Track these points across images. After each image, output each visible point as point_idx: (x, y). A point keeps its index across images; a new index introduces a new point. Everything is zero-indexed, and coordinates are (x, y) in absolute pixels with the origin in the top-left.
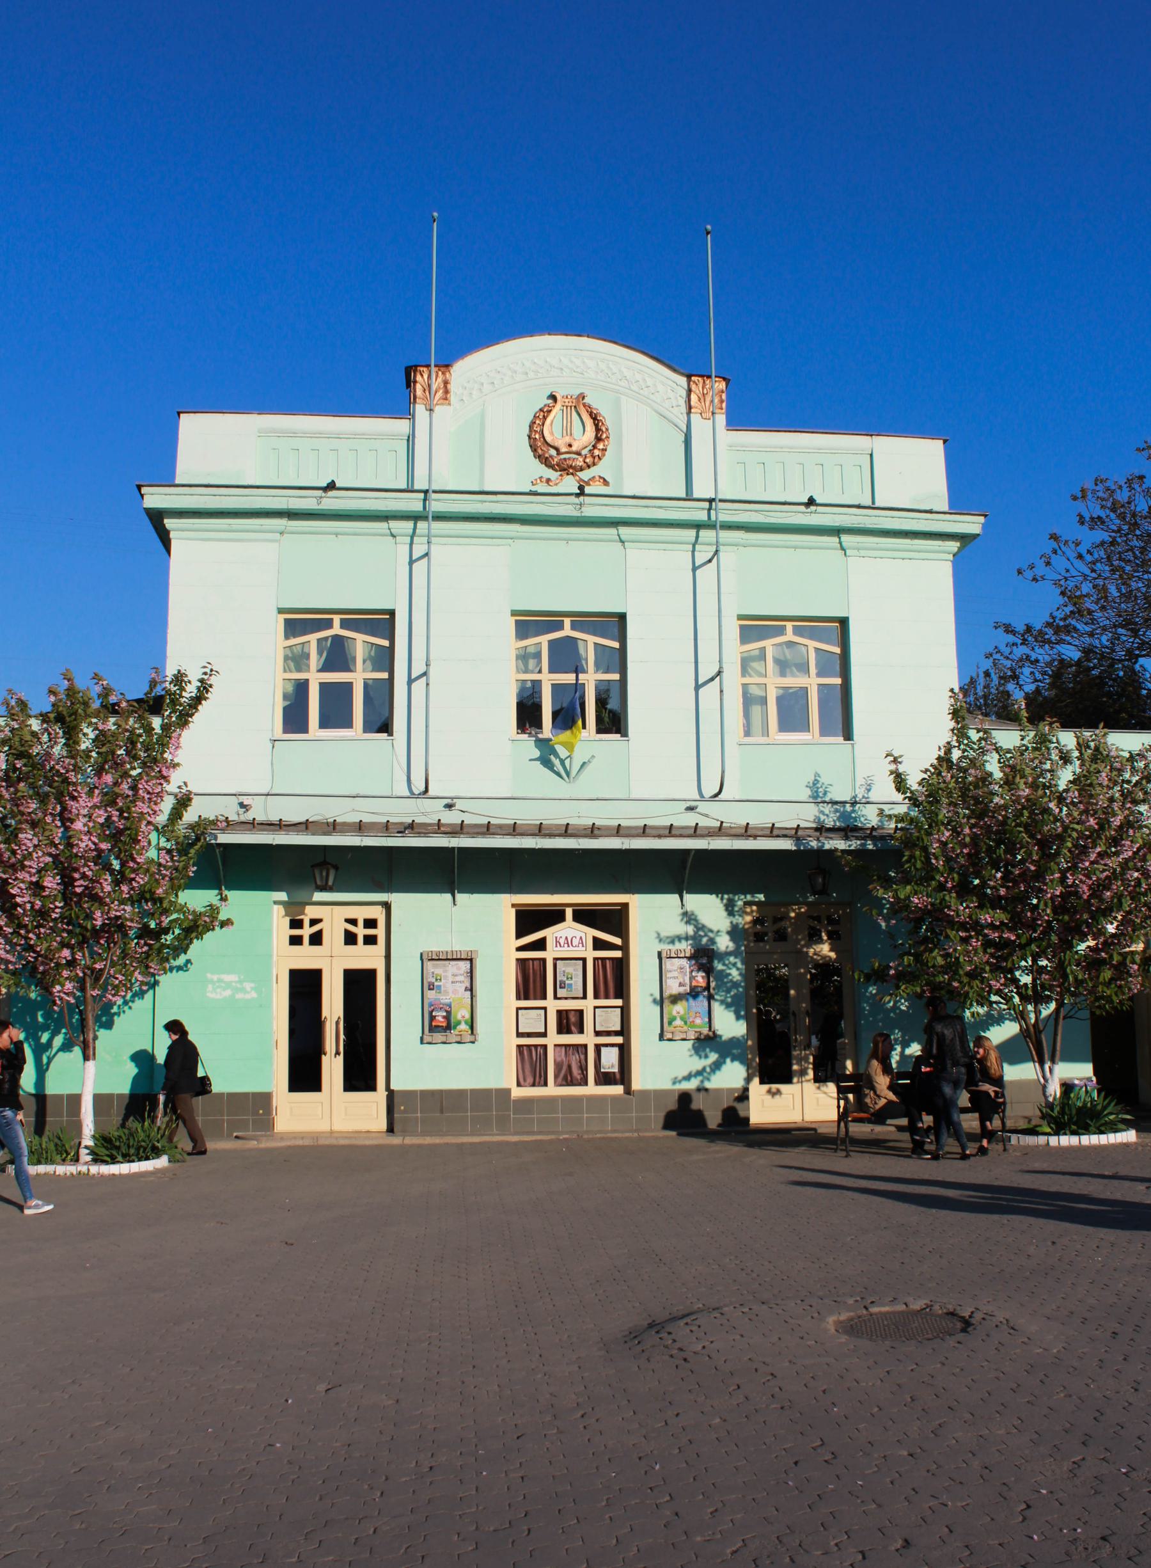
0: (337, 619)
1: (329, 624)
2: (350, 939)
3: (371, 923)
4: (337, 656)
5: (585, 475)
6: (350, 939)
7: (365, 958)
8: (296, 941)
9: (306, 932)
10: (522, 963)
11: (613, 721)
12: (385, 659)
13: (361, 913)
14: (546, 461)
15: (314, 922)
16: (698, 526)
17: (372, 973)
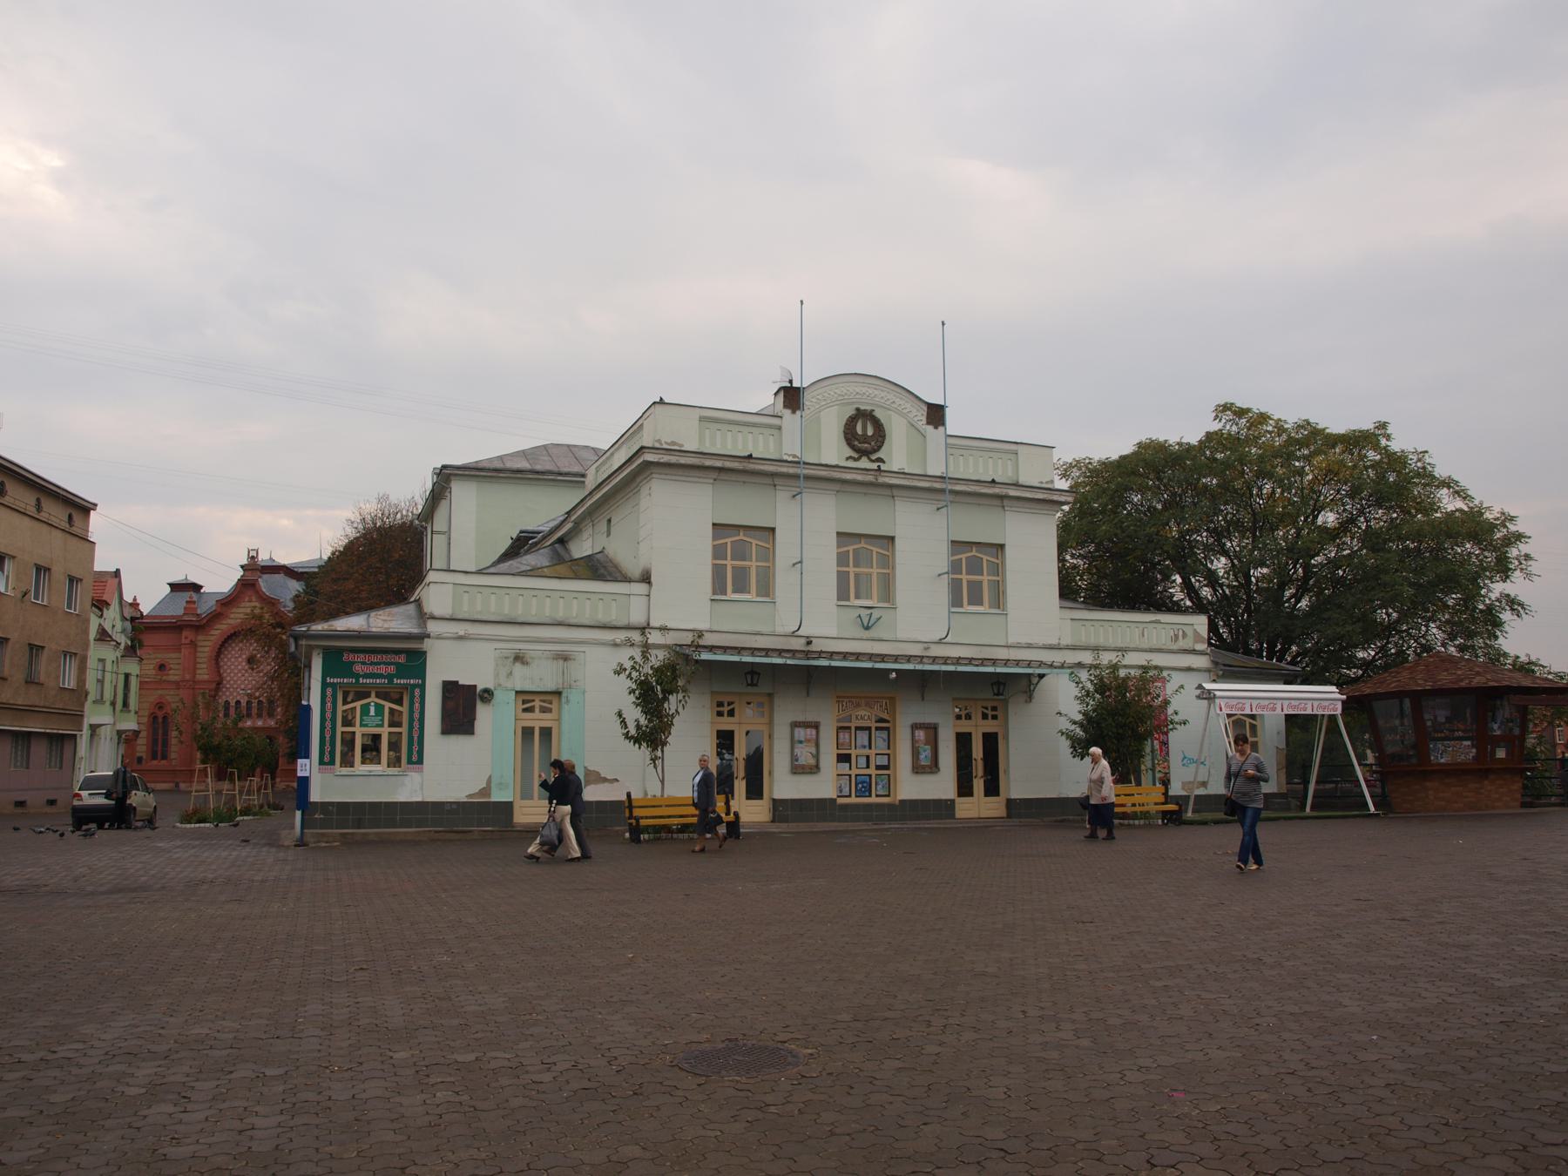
4: (741, 553)
5: (874, 457)
8: (720, 714)
9: (726, 709)
12: (768, 554)
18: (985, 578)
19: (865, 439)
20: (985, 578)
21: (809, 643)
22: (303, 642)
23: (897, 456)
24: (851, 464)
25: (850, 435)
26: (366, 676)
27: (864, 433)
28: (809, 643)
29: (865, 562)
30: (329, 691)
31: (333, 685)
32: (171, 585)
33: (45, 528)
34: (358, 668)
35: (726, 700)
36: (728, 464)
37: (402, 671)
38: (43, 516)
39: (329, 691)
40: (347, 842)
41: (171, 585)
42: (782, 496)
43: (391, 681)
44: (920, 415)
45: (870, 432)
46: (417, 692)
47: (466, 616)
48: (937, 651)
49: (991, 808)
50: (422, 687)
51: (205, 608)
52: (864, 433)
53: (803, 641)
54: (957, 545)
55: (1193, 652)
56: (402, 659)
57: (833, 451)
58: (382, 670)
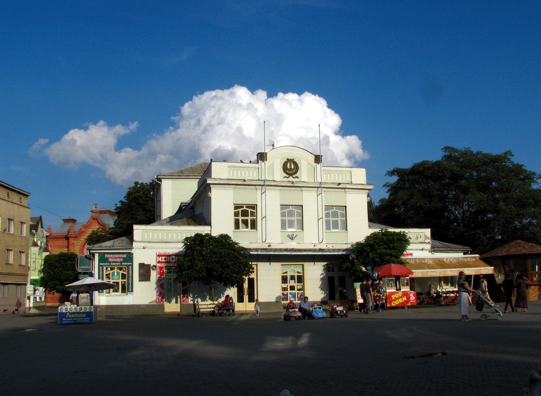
0: (245, 206)
1: (243, 207)
5: (294, 176)
10: (282, 276)
14: (286, 173)
16: (318, 187)
17: (253, 278)
18: (339, 219)
19: (291, 169)
20: (339, 219)
21: (269, 246)
23: (304, 175)
25: (285, 168)
26: (113, 262)
27: (291, 168)
28: (269, 246)
29: (292, 215)
30: (101, 268)
31: (102, 266)
32: (64, 220)
33: (11, 204)
34: (110, 260)
36: (238, 183)
37: (125, 260)
38: (11, 200)
39: (101, 268)
41: (64, 220)
43: (121, 264)
44: (313, 158)
45: (293, 167)
46: (130, 267)
47: (147, 241)
48: (318, 247)
50: (132, 265)
51: (77, 228)
52: (291, 168)
53: (268, 245)
54: (328, 207)
56: (125, 256)
57: (279, 175)
58: (119, 260)
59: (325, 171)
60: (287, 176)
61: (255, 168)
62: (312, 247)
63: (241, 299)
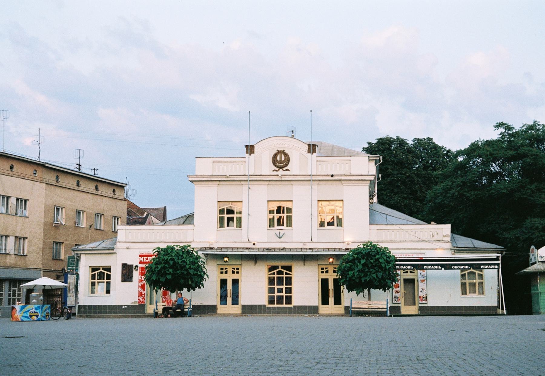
2: (233, 272)
3: (238, 269)
5: (285, 169)
6: (233, 272)
7: (235, 276)
8: (222, 273)
9: (224, 271)
11: (289, 224)
13: (236, 267)
15: (226, 269)
19: (281, 162)
22: (76, 252)
23: (294, 167)
24: (275, 173)
27: (281, 160)
35: (224, 267)
36: (220, 179)
40: (87, 317)
42: (245, 188)
45: (283, 159)
49: (237, 310)
52: (281, 160)
55: (445, 242)
57: (268, 168)
59: (320, 161)
60: (277, 169)
61: (242, 162)
62: (301, 246)
63: (325, 301)
